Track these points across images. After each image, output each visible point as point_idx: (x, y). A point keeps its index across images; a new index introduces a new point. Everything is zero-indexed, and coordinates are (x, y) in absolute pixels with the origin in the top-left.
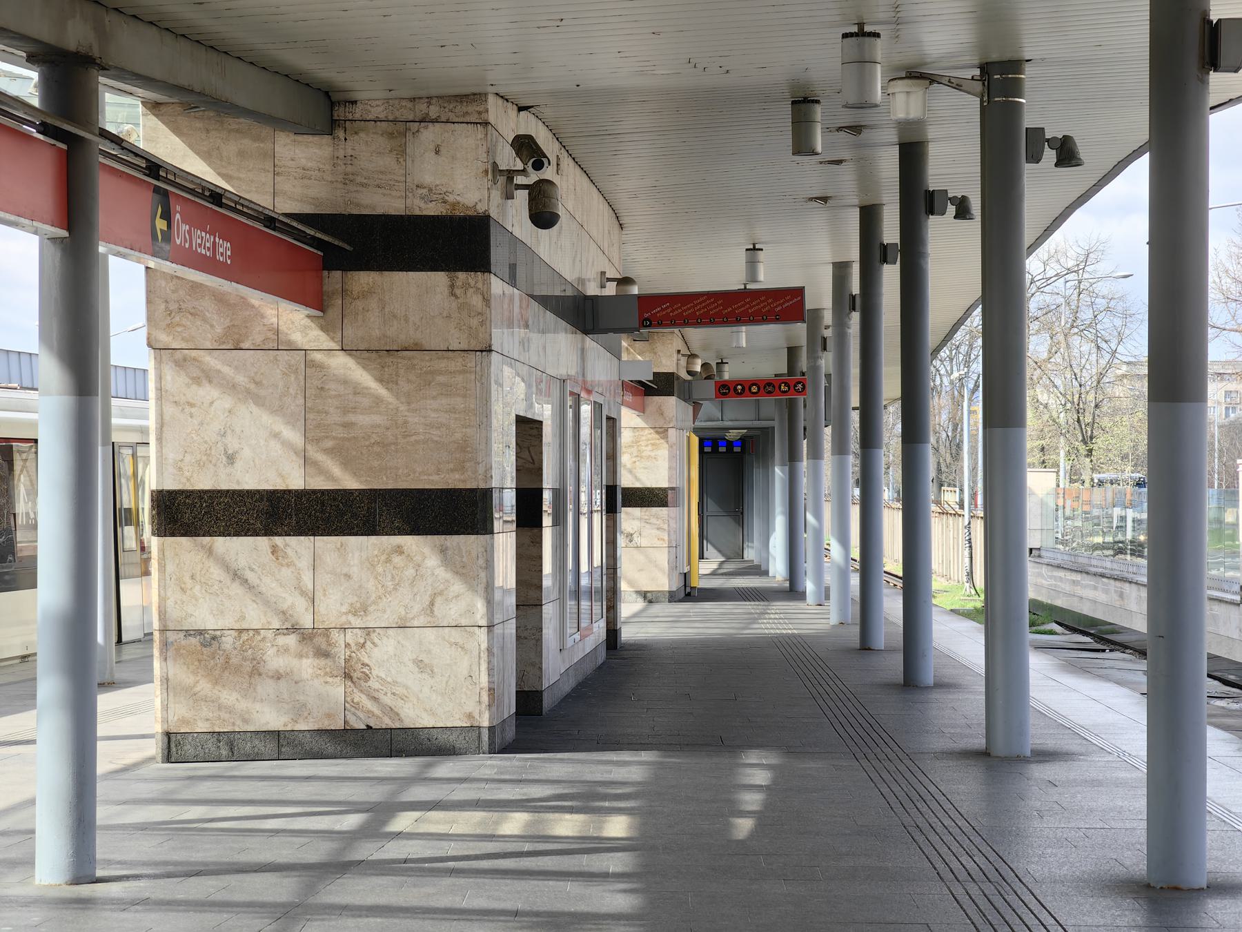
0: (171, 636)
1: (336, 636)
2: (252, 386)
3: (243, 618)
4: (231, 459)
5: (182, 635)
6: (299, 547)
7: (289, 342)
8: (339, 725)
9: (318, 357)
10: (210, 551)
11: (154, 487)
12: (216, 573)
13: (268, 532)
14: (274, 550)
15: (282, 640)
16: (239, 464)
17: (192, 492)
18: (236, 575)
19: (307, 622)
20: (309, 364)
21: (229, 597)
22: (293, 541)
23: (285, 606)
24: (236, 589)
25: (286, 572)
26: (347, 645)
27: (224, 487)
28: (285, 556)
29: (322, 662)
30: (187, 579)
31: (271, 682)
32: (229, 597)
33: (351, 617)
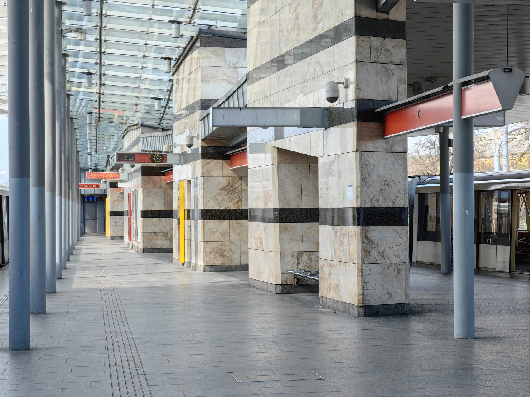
0: (144, 233)
1: (168, 233)
2: (157, 194)
3: (155, 231)
4: (153, 206)
6: (163, 219)
8: (169, 248)
11: (110, 210)
14: (160, 220)
15: (160, 234)
16: (155, 206)
21: (153, 227)
22: (162, 218)
26: (170, 235)
27: (152, 210)
28: (161, 221)
30: (147, 224)
31: (159, 241)
32: (153, 227)
33: (171, 231)
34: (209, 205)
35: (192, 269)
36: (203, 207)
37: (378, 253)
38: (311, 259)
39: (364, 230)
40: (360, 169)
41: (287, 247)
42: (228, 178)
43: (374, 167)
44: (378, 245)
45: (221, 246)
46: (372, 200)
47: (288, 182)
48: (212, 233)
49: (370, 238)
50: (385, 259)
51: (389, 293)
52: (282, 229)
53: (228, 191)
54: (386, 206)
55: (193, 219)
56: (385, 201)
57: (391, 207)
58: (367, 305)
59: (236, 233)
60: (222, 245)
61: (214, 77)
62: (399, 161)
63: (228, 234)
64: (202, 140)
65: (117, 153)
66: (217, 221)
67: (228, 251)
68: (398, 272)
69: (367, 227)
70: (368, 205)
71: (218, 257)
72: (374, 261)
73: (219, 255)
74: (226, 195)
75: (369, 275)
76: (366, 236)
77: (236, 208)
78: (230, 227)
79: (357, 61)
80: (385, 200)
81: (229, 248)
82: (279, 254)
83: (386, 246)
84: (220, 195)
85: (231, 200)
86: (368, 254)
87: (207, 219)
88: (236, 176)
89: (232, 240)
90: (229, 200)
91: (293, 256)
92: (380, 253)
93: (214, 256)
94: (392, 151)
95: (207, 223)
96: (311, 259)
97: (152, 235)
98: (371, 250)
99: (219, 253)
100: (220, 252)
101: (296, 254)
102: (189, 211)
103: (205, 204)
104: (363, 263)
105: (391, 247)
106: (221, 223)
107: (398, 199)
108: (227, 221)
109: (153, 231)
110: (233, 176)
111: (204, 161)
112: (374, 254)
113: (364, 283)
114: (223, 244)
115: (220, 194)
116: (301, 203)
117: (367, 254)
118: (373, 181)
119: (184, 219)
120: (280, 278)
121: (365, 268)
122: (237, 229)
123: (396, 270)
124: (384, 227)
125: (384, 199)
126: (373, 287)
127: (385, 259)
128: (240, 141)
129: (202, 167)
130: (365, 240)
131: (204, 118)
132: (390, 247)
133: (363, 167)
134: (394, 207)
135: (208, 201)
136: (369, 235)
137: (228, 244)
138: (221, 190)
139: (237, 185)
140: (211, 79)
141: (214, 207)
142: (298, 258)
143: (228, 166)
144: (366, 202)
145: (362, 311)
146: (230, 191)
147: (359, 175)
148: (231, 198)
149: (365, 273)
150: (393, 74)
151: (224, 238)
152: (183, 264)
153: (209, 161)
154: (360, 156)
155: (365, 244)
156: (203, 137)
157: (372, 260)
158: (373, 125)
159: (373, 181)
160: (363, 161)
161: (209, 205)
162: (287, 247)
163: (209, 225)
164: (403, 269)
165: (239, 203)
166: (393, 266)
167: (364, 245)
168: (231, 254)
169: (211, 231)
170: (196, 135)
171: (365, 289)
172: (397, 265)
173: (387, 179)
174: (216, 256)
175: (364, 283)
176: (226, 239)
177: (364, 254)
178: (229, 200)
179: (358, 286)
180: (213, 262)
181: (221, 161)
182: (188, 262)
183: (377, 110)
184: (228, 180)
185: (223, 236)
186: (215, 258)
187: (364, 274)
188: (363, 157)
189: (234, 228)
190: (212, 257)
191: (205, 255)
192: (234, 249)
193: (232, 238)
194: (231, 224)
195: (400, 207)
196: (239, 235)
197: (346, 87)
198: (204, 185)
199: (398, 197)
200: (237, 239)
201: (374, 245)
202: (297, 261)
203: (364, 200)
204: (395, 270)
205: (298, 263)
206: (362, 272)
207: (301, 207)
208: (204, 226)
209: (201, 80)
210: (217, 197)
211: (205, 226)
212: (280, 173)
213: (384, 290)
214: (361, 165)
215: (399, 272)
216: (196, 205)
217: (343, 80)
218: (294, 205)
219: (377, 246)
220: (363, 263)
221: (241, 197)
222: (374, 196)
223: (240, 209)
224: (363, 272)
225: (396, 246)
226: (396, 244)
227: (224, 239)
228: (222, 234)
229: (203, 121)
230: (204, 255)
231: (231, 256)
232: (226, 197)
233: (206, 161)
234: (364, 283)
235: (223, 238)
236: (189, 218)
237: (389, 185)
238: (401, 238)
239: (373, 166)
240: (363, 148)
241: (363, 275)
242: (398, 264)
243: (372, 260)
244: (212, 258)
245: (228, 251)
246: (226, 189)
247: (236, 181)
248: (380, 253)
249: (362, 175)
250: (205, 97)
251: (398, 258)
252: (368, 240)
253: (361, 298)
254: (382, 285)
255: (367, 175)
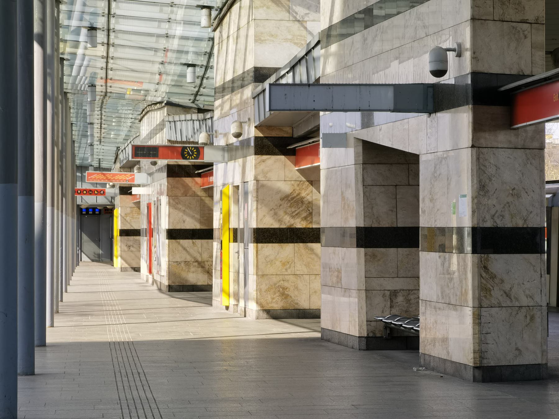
0: (170, 263)
1: (206, 263)
2: (189, 205)
3: (186, 259)
4: (184, 222)
5: (173, 262)
6: (198, 242)
7: (197, 195)
8: (206, 284)
9: (203, 198)
10: (179, 243)
12: (180, 248)
13: (192, 238)
14: (193, 243)
16: (186, 223)
17: (176, 229)
18: (185, 249)
19: (200, 260)
20: (202, 200)
23: (195, 256)
24: (184, 252)
25: (196, 248)
26: (208, 265)
27: (183, 228)
28: (195, 244)
29: (203, 269)
30: (174, 249)
34: (264, 222)
35: (241, 315)
36: (257, 224)
37: (502, 292)
38: (409, 300)
39: (482, 259)
40: (477, 172)
41: (375, 283)
42: (292, 182)
43: (496, 170)
44: (502, 281)
45: (282, 282)
46: (494, 216)
47: (376, 189)
48: (269, 263)
49: (490, 270)
50: (511, 301)
51: (517, 349)
52: (368, 257)
53: (292, 202)
54: (515, 226)
55: (242, 241)
56: (512, 218)
57: (521, 226)
58: (486, 365)
59: (304, 263)
60: (284, 280)
61: (273, 36)
62: (533, 161)
63: (291, 263)
64: (256, 127)
65: (133, 146)
66: (276, 245)
67: (292, 289)
68: (530, 320)
69: (486, 255)
70: (489, 224)
71: (278, 297)
72: (496, 303)
73: (279, 295)
74: (290, 207)
75: (489, 323)
76: (485, 268)
77: (304, 227)
78: (296, 254)
79: (473, 19)
80: (512, 216)
81: (293, 284)
82: (363, 294)
83: (513, 282)
84: (281, 207)
85: (297, 214)
86: (488, 293)
87: (262, 242)
88: (304, 179)
89: (298, 273)
90: (294, 214)
91: (384, 296)
92: (505, 293)
93: (272, 296)
94: (523, 147)
95: (262, 248)
96: (409, 300)
97: (183, 264)
98: (492, 288)
99: (279, 291)
100: (281, 289)
101: (388, 293)
102: (235, 231)
103: (259, 220)
104: (481, 306)
105: (521, 283)
106: (282, 248)
107: (531, 216)
108: (291, 246)
109: (183, 259)
110: (300, 179)
111: (258, 158)
112: (496, 293)
113: (482, 335)
114: (285, 279)
115: (281, 205)
116: (395, 220)
117: (486, 293)
118: (496, 189)
119: (229, 242)
120: (365, 327)
121: (483, 313)
122: (305, 257)
123: (528, 317)
124: (512, 255)
125: (512, 215)
126: (494, 340)
127: (511, 301)
128: (310, 128)
129: (255, 166)
130: (484, 273)
131: (258, 95)
132: (519, 284)
133: (481, 169)
134: (525, 226)
135: (264, 216)
136: (489, 267)
137: (292, 278)
138: (282, 199)
139: (306, 193)
140: (269, 38)
141: (272, 225)
142: (391, 299)
143: (292, 165)
144: (485, 220)
145: (478, 373)
146: (295, 202)
147: (475, 181)
148: (296, 212)
149: (483, 320)
150: (526, 37)
151: (286, 270)
152: (227, 308)
153: (265, 157)
154: (478, 154)
155: (484, 279)
156: (257, 123)
157: (494, 302)
158: (497, 110)
159: (496, 189)
160: (481, 160)
161: (264, 222)
162: (375, 283)
163: (264, 251)
164: (538, 314)
165: (309, 219)
166: (524, 310)
167: (483, 281)
168: (296, 293)
169: (268, 260)
170: (247, 120)
171: (484, 343)
172: (530, 309)
173: (516, 187)
174: (274, 296)
175: (482, 335)
176: (289, 272)
177: (482, 293)
178: (294, 214)
179: (474, 338)
180: (270, 305)
181: (283, 157)
182: (234, 305)
183: (503, 89)
184: (293, 185)
185: (285, 267)
186: (273, 299)
187: (482, 322)
188: (481, 156)
189: (301, 256)
190: (270, 297)
191: (259, 294)
192: (300, 285)
193: (297, 270)
194: (296, 249)
195: (535, 226)
196: (307, 265)
197: (459, 55)
198: (257, 192)
199: (531, 212)
200: (306, 271)
201: (497, 281)
202: (389, 303)
203: (483, 216)
204: (526, 317)
205: (391, 307)
206: (478, 318)
207: (395, 226)
208: (257, 252)
209: (255, 40)
210: (276, 211)
211: (259, 252)
212: (365, 176)
213: (510, 344)
214: (478, 167)
215: (532, 320)
216: (246, 222)
217: (455, 46)
218: (385, 223)
219: (500, 282)
220: (481, 307)
221: (311, 211)
222: (497, 211)
223: (309, 228)
224: (480, 319)
225: (529, 282)
226: (528, 280)
227: (287, 271)
228: (284, 264)
229: (256, 99)
230: (257, 294)
231: (297, 296)
232: (290, 209)
233: (260, 159)
234: (483, 334)
235: (284, 270)
236: (235, 240)
237: (518, 196)
238: (535, 271)
239: (495, 168)
240: (483, 142)
241: (481, 323)
242: (531, 308)
243: (493, 301)
244: (269, 298)
245: (292, 289)
246: (289, 199)
247: (304, 187)
248: (505, 293)
249: (480, 181)
250: (259, 65)
251: (531, 299)
252: (489, 273)
253: (477, 355)
254: (508, 338)
255: (488, 181)
